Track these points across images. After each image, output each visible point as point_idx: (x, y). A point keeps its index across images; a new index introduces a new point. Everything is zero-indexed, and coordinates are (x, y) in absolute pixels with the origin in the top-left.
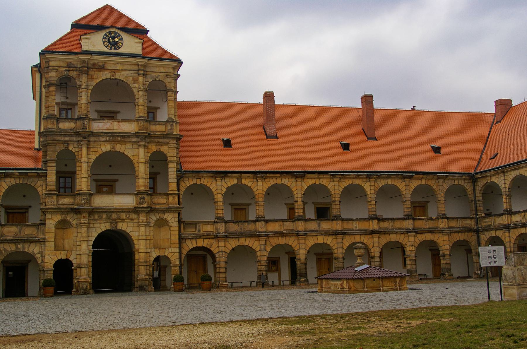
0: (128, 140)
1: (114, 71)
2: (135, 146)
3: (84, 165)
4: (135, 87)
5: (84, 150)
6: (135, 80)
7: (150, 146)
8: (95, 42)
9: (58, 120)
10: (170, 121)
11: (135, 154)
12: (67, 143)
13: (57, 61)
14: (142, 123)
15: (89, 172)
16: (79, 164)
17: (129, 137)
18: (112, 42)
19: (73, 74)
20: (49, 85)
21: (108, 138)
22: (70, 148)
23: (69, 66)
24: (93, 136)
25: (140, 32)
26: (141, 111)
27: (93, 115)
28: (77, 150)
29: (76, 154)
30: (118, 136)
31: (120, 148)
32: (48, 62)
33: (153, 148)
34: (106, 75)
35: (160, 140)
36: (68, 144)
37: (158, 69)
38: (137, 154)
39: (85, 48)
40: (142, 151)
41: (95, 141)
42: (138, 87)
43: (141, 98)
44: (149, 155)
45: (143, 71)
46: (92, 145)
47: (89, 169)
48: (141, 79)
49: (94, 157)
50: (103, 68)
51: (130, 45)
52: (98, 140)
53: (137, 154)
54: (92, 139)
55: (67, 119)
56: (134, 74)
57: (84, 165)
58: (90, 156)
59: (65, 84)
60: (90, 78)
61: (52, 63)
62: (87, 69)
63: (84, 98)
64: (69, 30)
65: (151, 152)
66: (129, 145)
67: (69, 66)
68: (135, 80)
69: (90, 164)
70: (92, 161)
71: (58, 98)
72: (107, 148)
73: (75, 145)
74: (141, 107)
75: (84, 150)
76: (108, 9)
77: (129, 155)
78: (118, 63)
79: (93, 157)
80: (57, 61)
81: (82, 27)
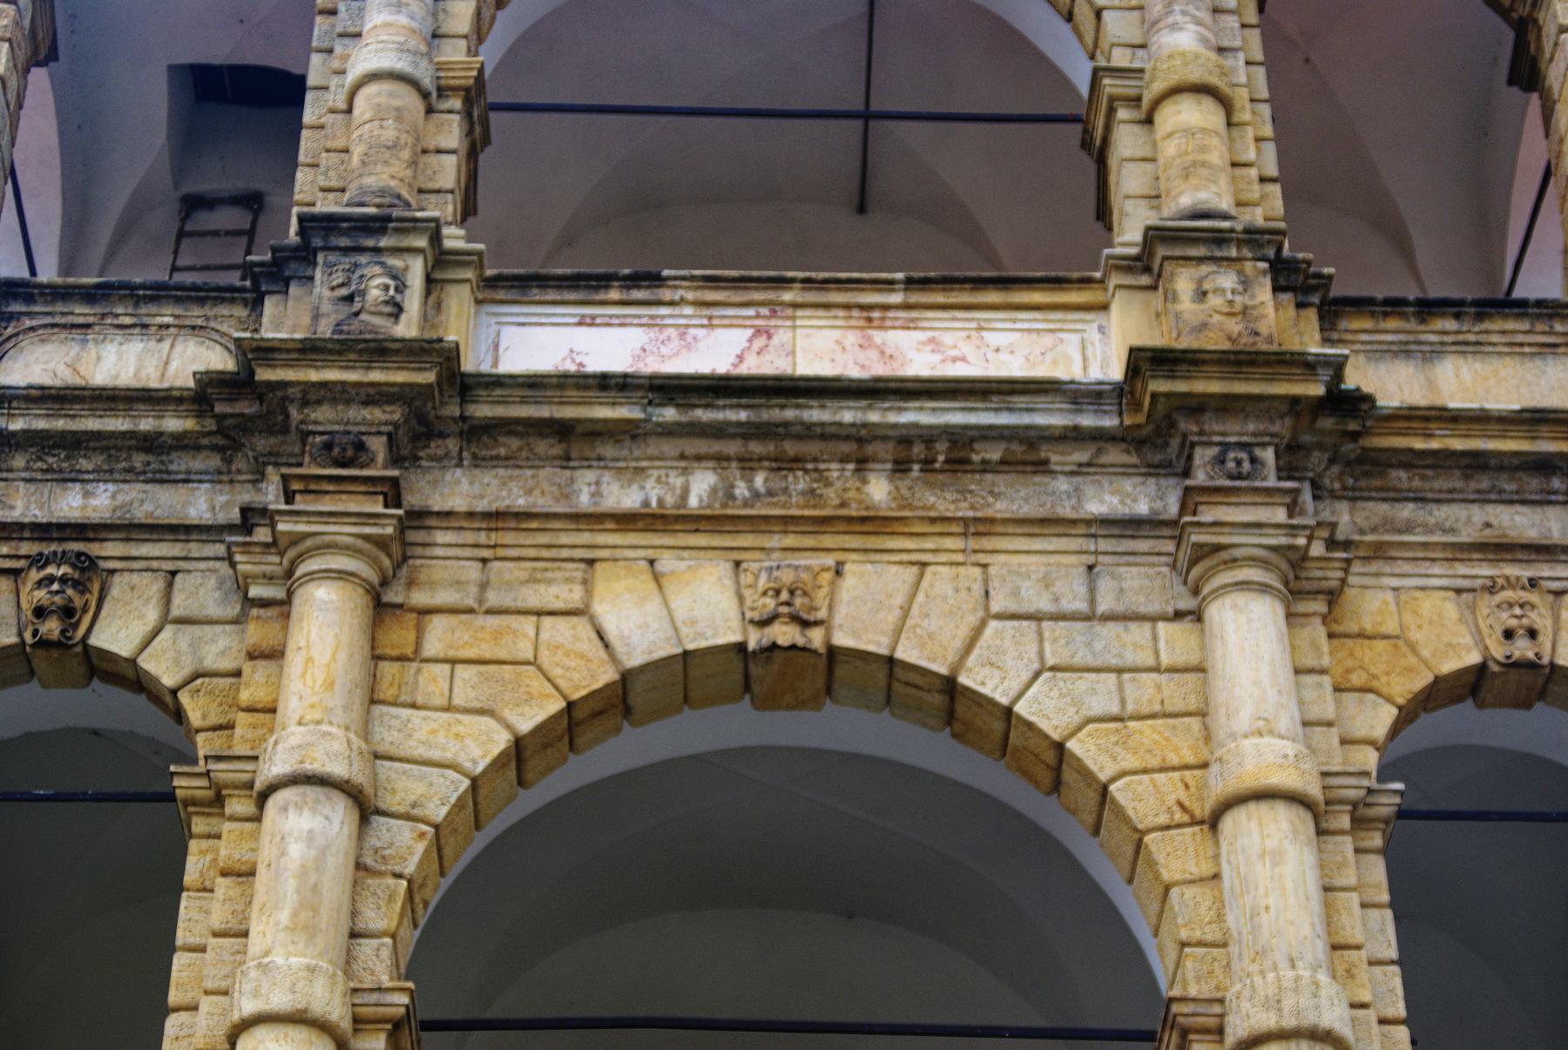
0: (1015, 498)
2: (1140, 581)
3: (303, 834)
5: (325, 620)
7: (1374, 601)
11: (1143, 692)
12: (77, 560)
15: (377, 962)
16: (231, 844)
17: (1028, 454)
21: (701, 487)
22: (116, 634)
24: (481, 441)
28: (220, 649)
29: (195, 709)
30: (859, 448)
31: (877, 604)
33: (1432, 623)
35: (1522, 523)
36: (88, 573)
38: (1178, 693)
40: (1248, 634)
41: (496, 518)
44: (1378, 719)
46: (447, 571)
47: (381, 914)
49: (482, 744)
52: (543, 502)
53: (1178, 693)
54: (457, 489)
57: (303, 834)
58: (418, 731)
65: (1407, 686)
66: (1034, 572)
69: (405, 845)
70: (438, 795)
72: (694, 604)
73: (202, 591)
74: (1189, 114)
75: (325, 620)
77: (1045, 709)
79: (453, 739)
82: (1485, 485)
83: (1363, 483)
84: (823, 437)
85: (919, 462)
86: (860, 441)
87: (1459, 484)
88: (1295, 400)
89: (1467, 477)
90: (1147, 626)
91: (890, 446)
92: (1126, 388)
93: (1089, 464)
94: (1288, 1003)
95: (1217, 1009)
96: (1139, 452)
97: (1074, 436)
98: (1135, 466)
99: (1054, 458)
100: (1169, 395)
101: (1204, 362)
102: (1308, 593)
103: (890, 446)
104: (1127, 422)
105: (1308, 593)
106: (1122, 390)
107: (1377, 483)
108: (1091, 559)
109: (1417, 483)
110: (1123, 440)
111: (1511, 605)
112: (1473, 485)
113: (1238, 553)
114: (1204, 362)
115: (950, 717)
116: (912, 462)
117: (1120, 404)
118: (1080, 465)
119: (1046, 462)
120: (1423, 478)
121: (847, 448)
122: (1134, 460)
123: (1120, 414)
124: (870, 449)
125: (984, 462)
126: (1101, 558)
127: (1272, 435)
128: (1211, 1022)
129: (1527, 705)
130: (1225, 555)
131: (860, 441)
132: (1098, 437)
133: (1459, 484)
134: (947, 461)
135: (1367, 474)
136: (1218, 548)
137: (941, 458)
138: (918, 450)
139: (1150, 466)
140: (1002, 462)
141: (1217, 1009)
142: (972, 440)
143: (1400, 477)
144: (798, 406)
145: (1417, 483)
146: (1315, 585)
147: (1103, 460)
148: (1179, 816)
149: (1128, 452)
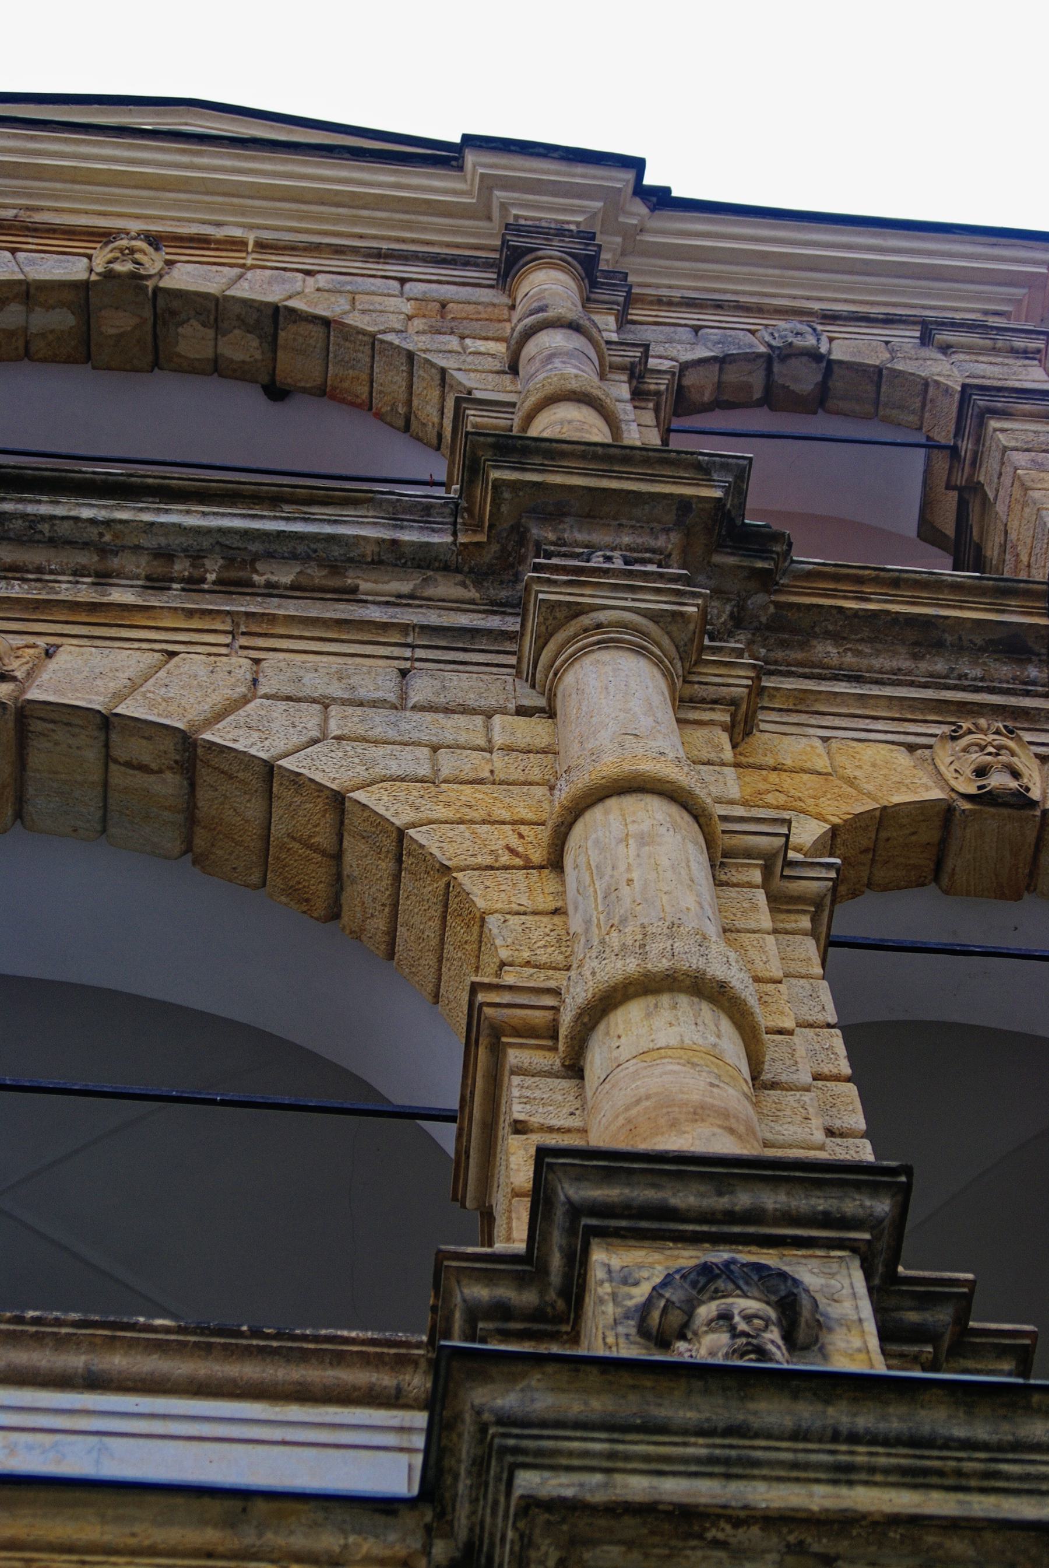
82: (940, 666)
83: (780, 655)
84: (52, 542)
85: (182, 580)
86: (104, 551)
87: (906, 664)
88: (684, 505)
89: (915, 657)
90: (479, 720)
91: (144, 560)
92: (464, 504)
93: (411, 596)
94: (654, 948)
95: (549, 1001)
96: (478, 584)
97: (392, 557)
98: (472, 602)
99: (364, 586)
100: (515, 486)
101: (563, 455)
102: (703, 701)
103: (144, 560)
104: (462, 539)
105: (703, 701)
106: (457, 505)
107: (799, 656)
108: (407, 665)
109: (849, 659)
110: (458, 570)
111: (982, 748)
112: (924, 666)
113: (603, 616)
114: (563, 455)
115: (194, 838)
116: (172, 580)
117: (455, 524)
118: (399, 596)
119: (355, 590)
120: (858, 653)
121: (83, 558)
122: (473, 594)
123: (455, 534)
124: (115, 563)
125: (269, 585)
126: (417, 664)
127: (653, 551)
128: (538, 1017)
129: (1019, 897)
130: (586, 620)
131: (104, 551)
132: (424, 561)
133: (906, 664)
134: (218, 582)
135: (784, 644)
136: (577, 611)
137: (211, 577)
138: (181, 567)
139: (493, 603)
140: (293, 587)
141: (549, 1001)
142: (256, 558)
143: (827, 651)
144: (20, 501)
145: (849, 659)
146: (711, 692)
147: (429, 592)
148: (505, 859)
149: (464, 585)
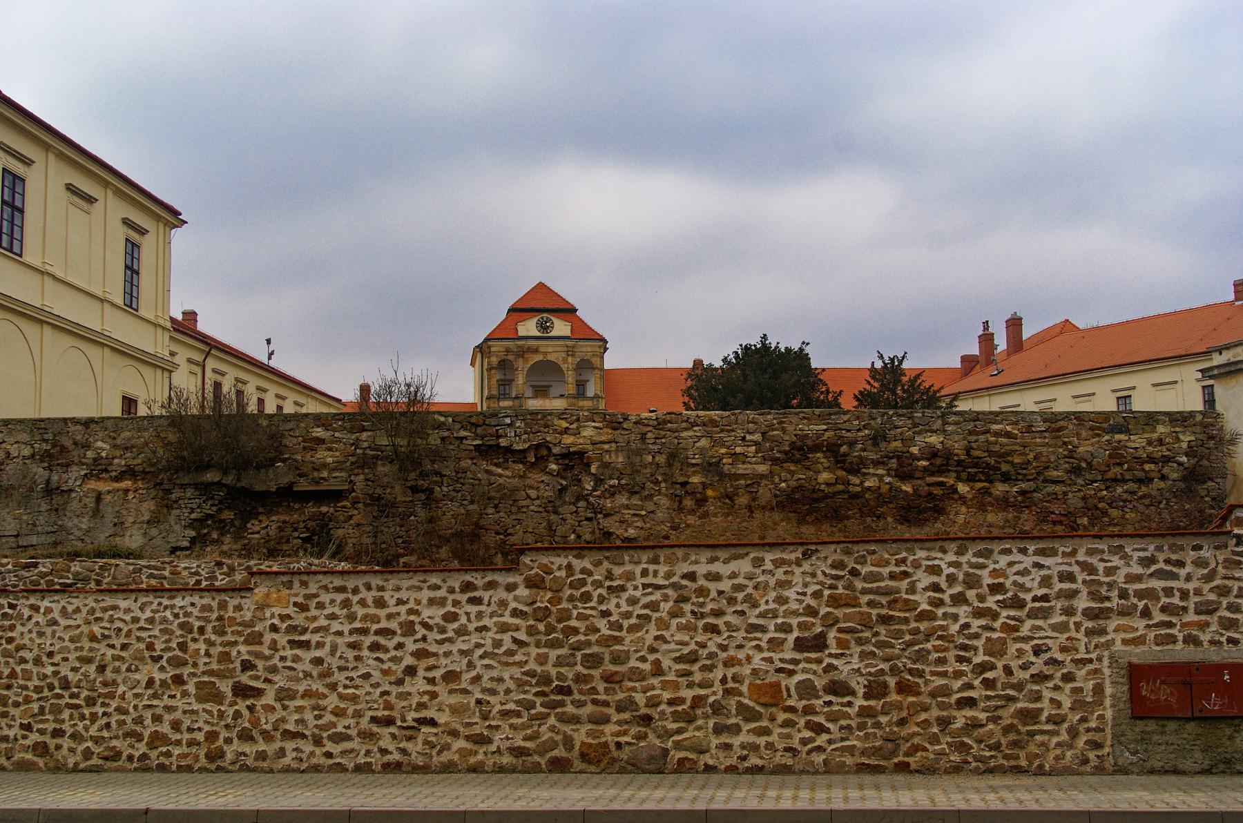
1: (545, 353)
4: (564, 367)
6: (565, 361)
8: (529, 328)
9: (499, 399)
10: (596, 397)
13: (497, 347)
14: (570, 400)
18: (543, 326)
19: (511, 357)
20: (489, 370)
23: (508, 350)
25: (568, 311)
26: (571, 389)
27: (529, 393)
32: (489, 347)
34: (538, 358)
37: (586, 349)
39: (520, 334)
42: (568, 366)
43: (571, 377)
45: (570, 352)
48: (570, 359)
50: (536, 351)
51: (561, 328)
55: (505, 399)
56: (563, 355)
59: (504, 365)
60: (526, 360)
61: (493, 349)
62: (522, 353)
63: (520, 379)
64: (504, 316)
67: (508, 350)
68: (565, 361)
71: (498, 375)
76: (541, 286)
78: (548, 346)
80: (497, 347)
81: (518, 311)
